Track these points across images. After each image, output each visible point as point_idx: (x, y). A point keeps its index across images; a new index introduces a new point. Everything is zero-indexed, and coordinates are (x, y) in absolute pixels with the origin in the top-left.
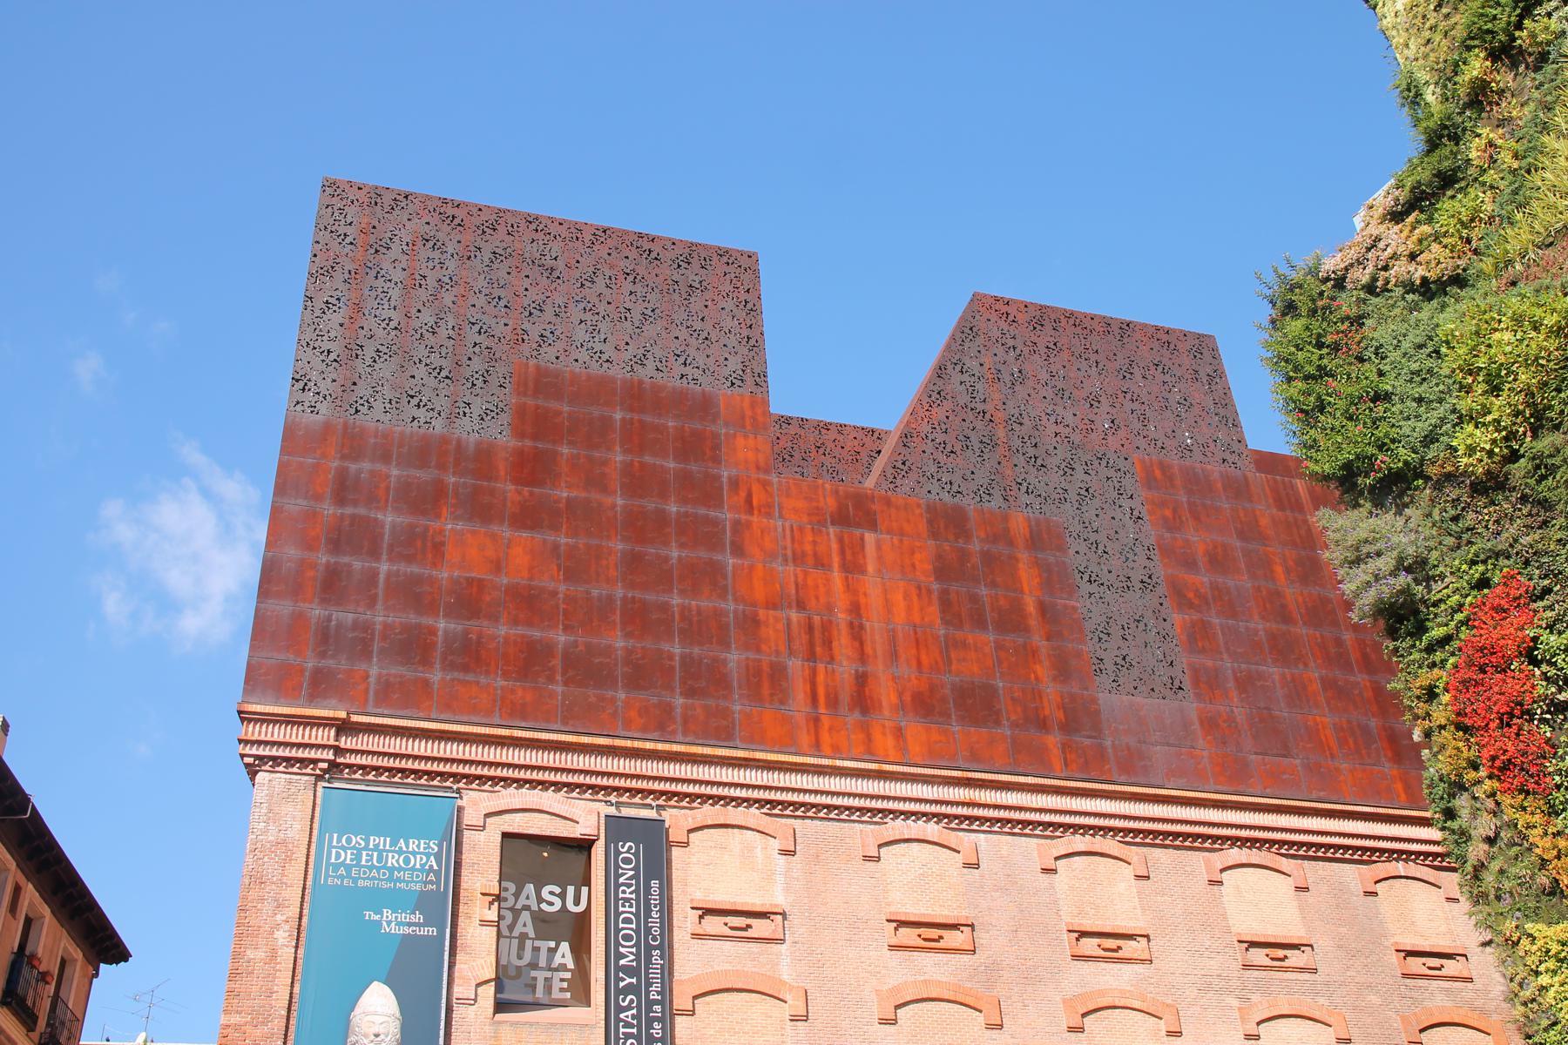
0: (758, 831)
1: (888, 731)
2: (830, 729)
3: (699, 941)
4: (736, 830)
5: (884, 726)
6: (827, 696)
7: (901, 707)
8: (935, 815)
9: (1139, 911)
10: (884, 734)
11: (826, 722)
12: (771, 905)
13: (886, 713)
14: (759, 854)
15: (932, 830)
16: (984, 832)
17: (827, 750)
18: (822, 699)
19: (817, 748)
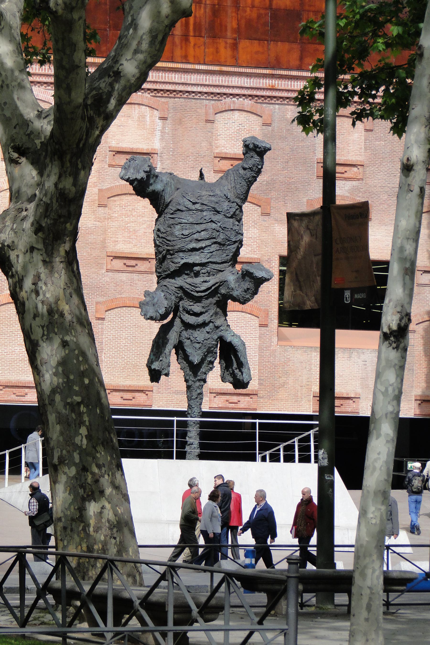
0: (149, 106)
1: (228, 45)
2: (195, 45)
3: (113, 168)
4: (136, 106)
5: (226, 43)
6: (195, 24)
7: (238, 31)
8: (250, 96)
9: (363, 150)
10: (226, 48)
11: (192, 39)
12: (152, 149)
13: (229, 34)
14: (148, 119)
15: (247, 103)
16: (278, 104)
17: (191, 60)
18: (191, 27)
19: (185, 59)
